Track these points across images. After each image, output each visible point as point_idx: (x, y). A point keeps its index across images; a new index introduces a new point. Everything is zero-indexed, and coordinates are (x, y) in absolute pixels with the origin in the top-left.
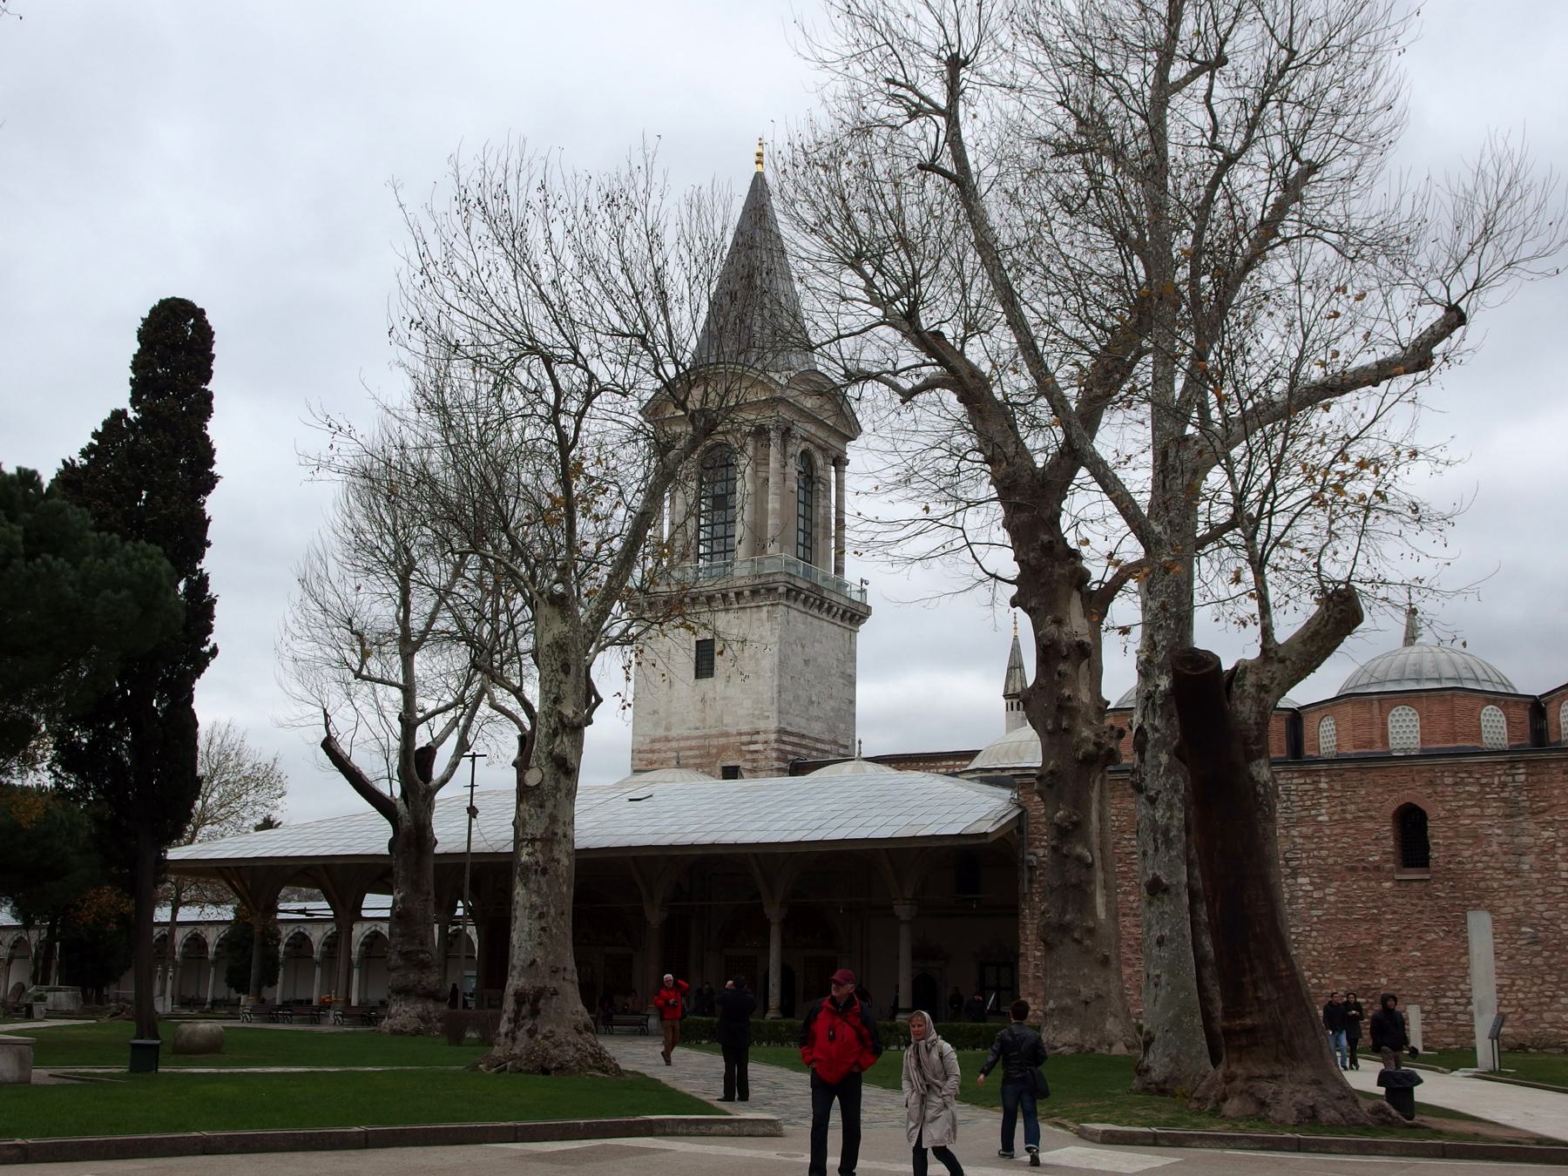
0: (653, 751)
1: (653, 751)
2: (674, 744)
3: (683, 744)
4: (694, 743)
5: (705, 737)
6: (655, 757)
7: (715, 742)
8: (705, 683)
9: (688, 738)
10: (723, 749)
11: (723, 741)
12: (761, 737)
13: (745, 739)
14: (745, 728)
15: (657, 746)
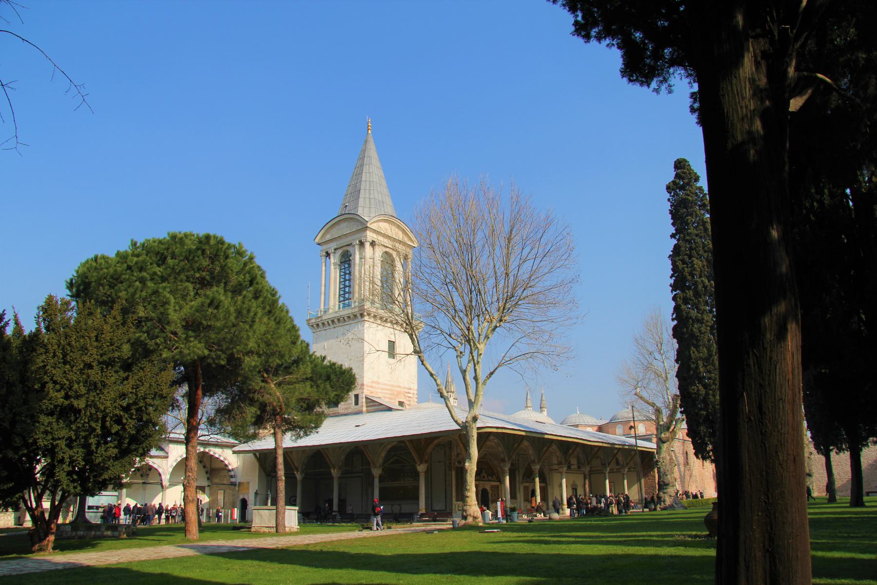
0: (372, 387)
1: (372, 387)
2: (381, 386)
3: (384, 387)
4: (388, 387)
5: (393, 386)
6: (373, 390)
7: (396, 389)
8: (392, 361)
9: (386, 385)
10: (399, 393)
11: (398, 389)
12: (411, 391)
13: (407, 390)
14: (407, 386)
15: (374, 385)
